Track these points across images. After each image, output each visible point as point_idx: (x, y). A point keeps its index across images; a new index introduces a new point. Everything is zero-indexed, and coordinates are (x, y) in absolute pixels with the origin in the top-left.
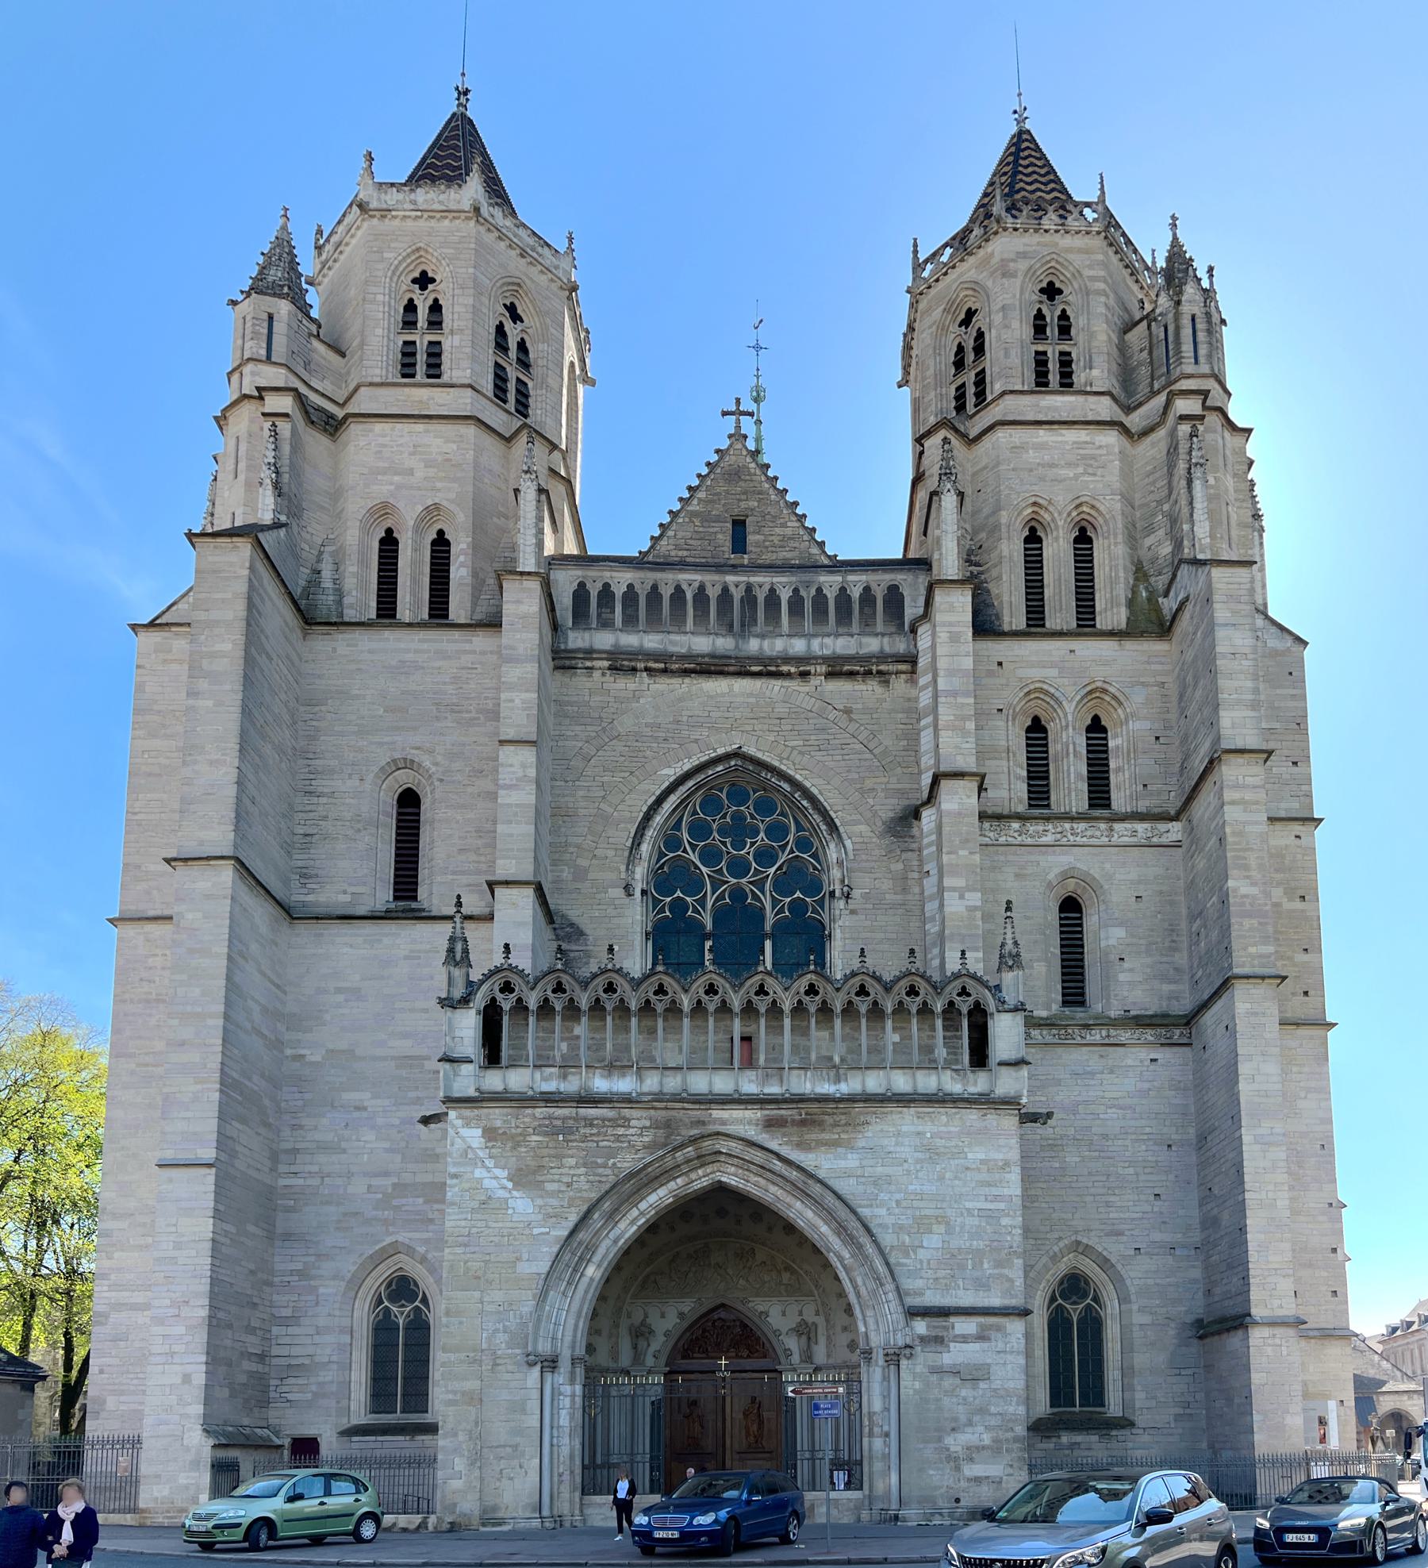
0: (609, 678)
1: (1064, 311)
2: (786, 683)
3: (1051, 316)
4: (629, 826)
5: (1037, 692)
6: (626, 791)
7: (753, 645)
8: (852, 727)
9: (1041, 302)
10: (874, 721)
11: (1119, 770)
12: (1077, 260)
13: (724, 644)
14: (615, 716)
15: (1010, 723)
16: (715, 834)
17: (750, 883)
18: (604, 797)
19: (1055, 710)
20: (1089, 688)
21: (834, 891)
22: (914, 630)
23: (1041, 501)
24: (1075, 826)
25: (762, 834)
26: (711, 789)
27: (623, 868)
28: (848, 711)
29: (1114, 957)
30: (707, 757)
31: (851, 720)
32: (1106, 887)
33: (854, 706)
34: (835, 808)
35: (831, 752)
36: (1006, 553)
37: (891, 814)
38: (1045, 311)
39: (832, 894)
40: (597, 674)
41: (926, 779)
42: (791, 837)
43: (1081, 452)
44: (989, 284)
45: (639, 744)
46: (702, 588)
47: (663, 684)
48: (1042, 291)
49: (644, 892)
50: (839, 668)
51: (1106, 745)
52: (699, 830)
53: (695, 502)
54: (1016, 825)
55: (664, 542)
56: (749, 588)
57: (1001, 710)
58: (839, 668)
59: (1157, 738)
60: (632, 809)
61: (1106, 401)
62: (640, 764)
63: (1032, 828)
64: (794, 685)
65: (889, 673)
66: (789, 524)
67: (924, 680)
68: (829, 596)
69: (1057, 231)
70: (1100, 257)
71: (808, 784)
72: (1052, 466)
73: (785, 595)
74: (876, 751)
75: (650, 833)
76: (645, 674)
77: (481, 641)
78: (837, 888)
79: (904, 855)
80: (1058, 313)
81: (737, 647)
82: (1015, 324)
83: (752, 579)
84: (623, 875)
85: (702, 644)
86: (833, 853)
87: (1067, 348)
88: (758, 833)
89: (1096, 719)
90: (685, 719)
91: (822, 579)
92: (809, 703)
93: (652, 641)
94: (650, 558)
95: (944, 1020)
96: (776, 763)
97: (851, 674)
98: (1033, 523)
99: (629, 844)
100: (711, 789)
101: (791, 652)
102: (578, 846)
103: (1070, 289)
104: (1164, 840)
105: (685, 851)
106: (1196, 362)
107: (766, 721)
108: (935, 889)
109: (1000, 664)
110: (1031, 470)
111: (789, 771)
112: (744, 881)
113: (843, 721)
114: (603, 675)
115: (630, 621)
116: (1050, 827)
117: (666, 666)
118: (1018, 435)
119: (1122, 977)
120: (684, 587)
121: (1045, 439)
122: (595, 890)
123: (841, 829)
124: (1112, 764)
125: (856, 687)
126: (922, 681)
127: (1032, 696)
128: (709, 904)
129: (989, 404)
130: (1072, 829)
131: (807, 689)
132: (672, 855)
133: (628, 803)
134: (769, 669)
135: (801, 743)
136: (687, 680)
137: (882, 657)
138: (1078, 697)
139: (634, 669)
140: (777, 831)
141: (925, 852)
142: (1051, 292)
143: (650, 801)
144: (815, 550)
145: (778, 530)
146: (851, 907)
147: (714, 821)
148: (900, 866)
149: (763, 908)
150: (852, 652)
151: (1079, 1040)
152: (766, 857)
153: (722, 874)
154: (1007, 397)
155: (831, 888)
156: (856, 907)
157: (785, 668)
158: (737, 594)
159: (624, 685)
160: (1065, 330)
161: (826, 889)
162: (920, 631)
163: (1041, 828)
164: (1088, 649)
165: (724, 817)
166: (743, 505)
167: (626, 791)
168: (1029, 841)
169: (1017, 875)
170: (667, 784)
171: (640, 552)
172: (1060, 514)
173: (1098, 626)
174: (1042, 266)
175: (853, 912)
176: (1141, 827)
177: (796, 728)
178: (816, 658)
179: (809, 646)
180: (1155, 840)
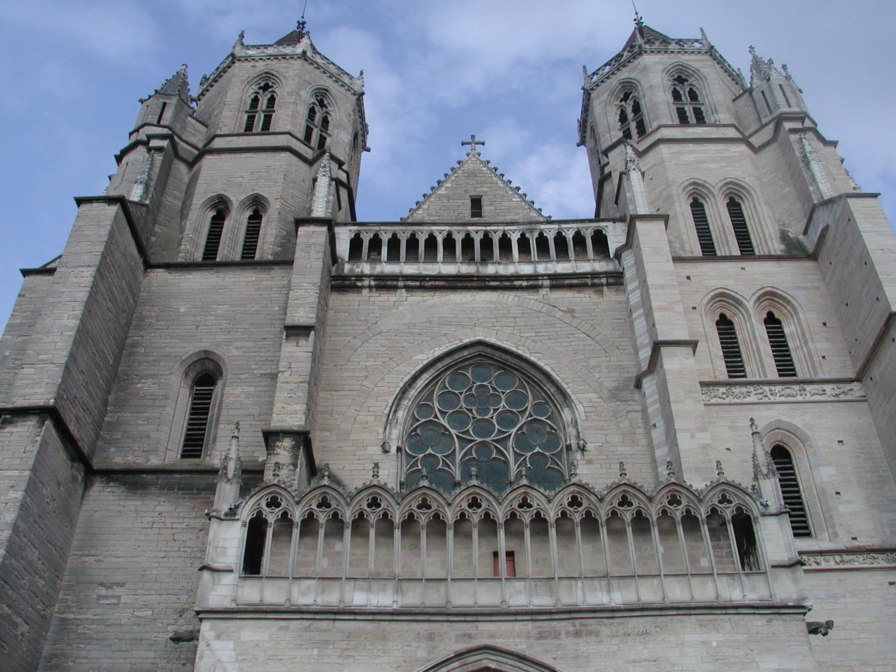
0: (375, 294)
1: (691, 89)
2: (519, 293)
3: (684, 91)
4: (387, 398)
5: (723, 297)
6: (386, 371)
7: (490, 269)
8: (575, 322)
9: (675, 85)
10: (593, 318)
11: (796, 348)
12: (695, 65)
13: (467, 269)
14: (378, 319)
15: (704, 317)
16: (462, 403)
17: (495, 441)
18: (366, 377)
19: (737, 308)
20: (761, 292)
21: (570, 445)
22: (618, 256)
23: (699, 181)
24: (773, 388)
25: (503, 403)
26: (459, 369)
27: (381, 430)
28: (571, 311)
29: (831, 491)
30: (455, 346)
31: (574, 317)
32: (809, 434)
33: (575, 308)
34: (566, 381)
35: (558, 340)
36: (679, 210)
37: (614, 384)
38: (678, 88)
39: (569, 448)
40: (365, 292)
41: (645, 353)
42: (529, 405)
43: (721, 155)
44: (639, 77)
45: (396, 338)
46: (450, 234)
47: (418, 298)
48: (674, 80)
49: (399, 449)
50: (558, 282)
51: (783, 332)
52: (448, 399)
53: (444, 189)
54: (723, 389)
55: (420, 212)
56: (486, 234)
57: (694, 308)
58: (558, 282)
59: (825, 324)
60: (390, 385)
61: (733, 130)
62: (398, 352)
63: (737, 390)
64: (525, 295)
65: (602, 285)
66: (514, 199)
67: (631, 285)
68: (548, 237)
69: (679, 52)
70: (710, 63)
71: (541, 364)
72: (703, 162)
73: (515, 238)
74: (597, 339)
75: (406, 403)
76: (404, 290)
77: (278, 273)
78: (573, 442)
79: (630, 416)
80: (688, 89)
81: (478, 271)
82: (661, 94)
83: (488, 228)
84: (381, 437)
85: (449, 269)
86: (566, 415)
87: (698, 106)
88: (499, 403)
89: (770, 314)
90: (436, 320)
91: (543, 227)
92: (538, 306)
93: (410, 269)
94: (410, 221)
95: (708, 524)
96: (514, 349)
97: (571, 287)
98: (695, 195)
99: (387, 411)
100: (459, 369)
101: (521, 273)
102: (343, 414)
103: (693, 78)
104: (848, 397)
105: (436, 417)
106: (790, 106)
107: (505, 319)
108: (664, 438)
109: (688, 278)
110: (688, 165)
111: (525, 354)
112: (488, 439)
113: (568, 318)
114: (370, 291)
115: (393, 256)
116: (752, 389)
117: (423, 284)
118: (675, 148)
119: (842, 508)
120: (436, 234)
121: (694, 149)
122: (355, 448)
123: (573, 397)
124: (791, 345)
125: (576, 295)
126: (630, 287)
127: (718, 299)
128: (458, 457)
129: (651, 134)
130: (771, 391)
131: (536, 297)
132: (424, 420)
133: (387, 380)
134: (506, 284)
135: (534, 334)
136: (437, 294)
137: (594, 275)
138: (755, 298)
139: (395, 288)
140: (517, 400)
141: (649, 410)
142: (681, 80)
143: (406, 379)
144: (533, 214)
145: (505, 203)
146: (586, 458)
147: (461, 393)
148: (626, 424)
149: (506, 463)
150: (571, 271)
151: (814, 566)
152: (507, 420)
153: (470, 435)
154: (662, 129)
155: (568, 443)
156: (592, 457)
157: (517, 283)
158: (477, 239)
159: (385, 298)
160: (693, 96)
161: (563, 444)
162: (624, 255)
163: (744, 389)
164: (753, 267)
165: (471, 389)
166: (478, 190)
167: (386, 371)
168: (736, 401)
169: (730, 428)
170: (420, 366)
171: (401, 219)
172: (714, 188)
173: (757, 253)
174: (673, 67)
175: (590, 462)
176: (828, 388)
177: (528, 323)
178: (542, 275)
179: (535, 269)
180: (842, 397)
